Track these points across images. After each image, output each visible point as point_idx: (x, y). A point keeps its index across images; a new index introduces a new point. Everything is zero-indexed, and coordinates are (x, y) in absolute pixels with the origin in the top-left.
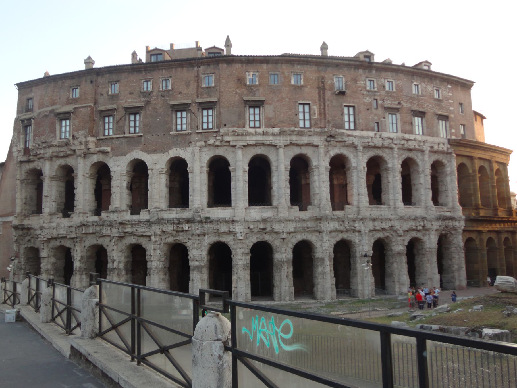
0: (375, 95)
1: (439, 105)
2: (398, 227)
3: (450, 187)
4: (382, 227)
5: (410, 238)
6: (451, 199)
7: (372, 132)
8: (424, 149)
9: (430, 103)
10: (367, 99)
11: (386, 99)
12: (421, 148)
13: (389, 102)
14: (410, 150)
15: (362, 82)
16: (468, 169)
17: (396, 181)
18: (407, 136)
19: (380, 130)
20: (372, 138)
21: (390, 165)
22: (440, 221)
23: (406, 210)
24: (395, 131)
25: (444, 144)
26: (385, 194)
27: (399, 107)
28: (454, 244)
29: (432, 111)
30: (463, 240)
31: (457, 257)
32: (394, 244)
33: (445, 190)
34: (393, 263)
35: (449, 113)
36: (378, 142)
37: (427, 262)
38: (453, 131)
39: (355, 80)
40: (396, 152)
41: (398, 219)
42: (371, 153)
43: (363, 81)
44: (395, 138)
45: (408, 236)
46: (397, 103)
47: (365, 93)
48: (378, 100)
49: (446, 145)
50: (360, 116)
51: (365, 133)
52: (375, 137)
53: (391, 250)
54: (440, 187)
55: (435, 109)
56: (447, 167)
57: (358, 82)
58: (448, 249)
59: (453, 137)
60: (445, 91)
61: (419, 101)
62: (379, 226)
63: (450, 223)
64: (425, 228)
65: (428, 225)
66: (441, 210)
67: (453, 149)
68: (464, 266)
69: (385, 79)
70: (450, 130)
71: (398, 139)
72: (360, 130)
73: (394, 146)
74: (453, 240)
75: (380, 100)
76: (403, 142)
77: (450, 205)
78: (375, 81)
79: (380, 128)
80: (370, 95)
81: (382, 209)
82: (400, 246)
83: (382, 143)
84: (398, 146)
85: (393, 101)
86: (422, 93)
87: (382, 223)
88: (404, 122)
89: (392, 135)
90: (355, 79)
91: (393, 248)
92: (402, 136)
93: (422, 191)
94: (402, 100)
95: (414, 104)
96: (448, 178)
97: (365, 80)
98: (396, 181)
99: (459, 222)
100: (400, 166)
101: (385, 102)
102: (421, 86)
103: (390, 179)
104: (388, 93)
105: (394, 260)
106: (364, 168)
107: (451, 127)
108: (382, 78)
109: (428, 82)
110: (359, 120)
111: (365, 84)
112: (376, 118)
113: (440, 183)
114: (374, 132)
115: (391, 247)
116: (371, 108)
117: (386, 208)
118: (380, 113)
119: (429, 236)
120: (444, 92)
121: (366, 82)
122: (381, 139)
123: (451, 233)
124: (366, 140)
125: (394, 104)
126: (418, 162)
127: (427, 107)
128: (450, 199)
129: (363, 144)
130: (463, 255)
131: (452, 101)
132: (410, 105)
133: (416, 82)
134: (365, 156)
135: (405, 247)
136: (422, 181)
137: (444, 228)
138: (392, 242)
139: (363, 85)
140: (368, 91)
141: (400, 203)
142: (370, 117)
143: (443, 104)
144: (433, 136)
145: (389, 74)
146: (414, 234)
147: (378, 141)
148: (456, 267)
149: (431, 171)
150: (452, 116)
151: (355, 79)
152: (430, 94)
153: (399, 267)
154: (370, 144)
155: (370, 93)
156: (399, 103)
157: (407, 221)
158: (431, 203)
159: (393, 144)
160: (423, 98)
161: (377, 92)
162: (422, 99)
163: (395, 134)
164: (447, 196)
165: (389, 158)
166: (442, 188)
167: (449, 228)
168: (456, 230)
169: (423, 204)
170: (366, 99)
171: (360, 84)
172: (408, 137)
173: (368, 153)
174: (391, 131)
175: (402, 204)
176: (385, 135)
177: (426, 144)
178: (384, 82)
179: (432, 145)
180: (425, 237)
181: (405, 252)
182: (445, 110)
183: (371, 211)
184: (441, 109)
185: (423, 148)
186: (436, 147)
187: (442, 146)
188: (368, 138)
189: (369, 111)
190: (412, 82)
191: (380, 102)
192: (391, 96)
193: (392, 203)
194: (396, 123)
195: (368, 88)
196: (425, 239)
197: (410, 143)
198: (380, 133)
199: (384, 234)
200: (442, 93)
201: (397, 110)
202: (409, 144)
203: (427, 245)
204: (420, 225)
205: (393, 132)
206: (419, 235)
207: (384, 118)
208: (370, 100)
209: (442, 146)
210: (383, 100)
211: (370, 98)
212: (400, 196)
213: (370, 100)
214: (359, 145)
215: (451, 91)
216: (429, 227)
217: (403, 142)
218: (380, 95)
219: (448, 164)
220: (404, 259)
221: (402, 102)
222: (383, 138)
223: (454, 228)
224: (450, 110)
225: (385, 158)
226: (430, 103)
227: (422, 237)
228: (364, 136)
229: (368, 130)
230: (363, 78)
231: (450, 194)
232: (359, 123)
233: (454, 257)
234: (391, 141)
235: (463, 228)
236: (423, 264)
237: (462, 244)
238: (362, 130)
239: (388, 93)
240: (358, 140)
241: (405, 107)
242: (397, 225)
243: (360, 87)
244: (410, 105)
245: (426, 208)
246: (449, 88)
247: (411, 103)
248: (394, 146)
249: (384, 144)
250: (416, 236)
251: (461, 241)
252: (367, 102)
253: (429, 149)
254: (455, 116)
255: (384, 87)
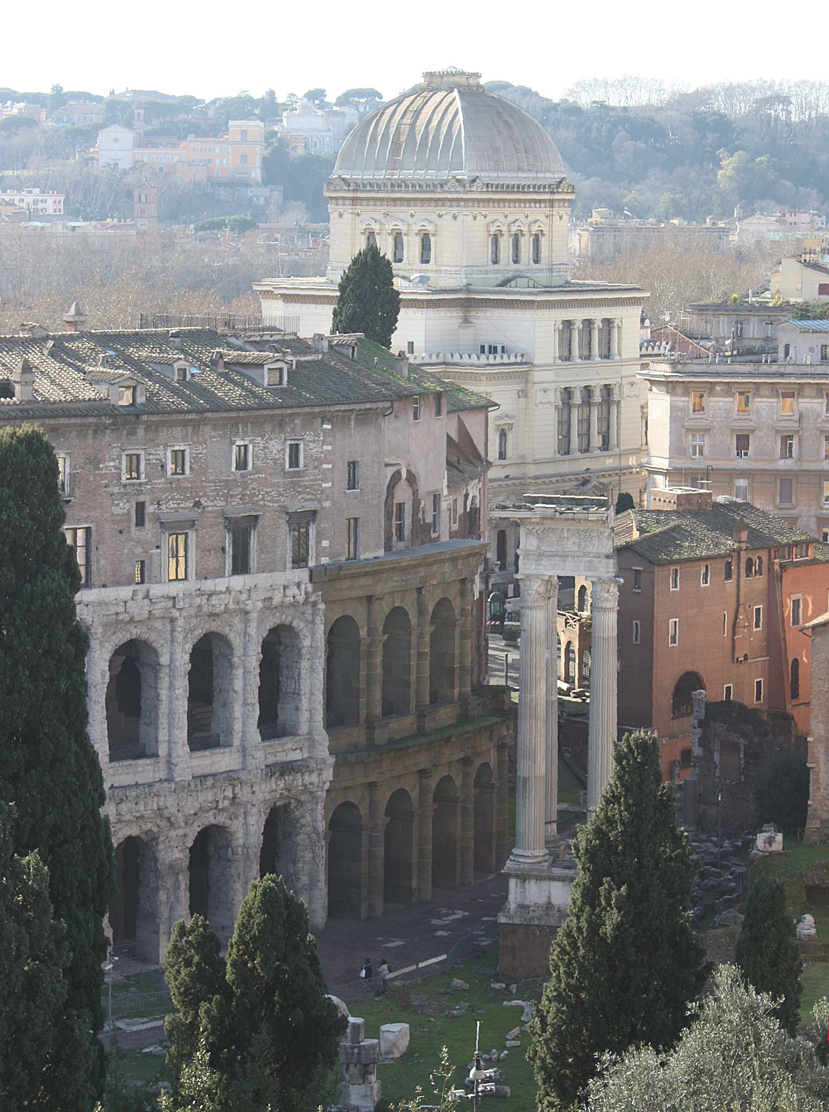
0: (139, 492)
1: (294, 485)
2: (173, 810)
3: (305, 687)
4: (138, 815)
5: (199, 829)
6: (307, 715)
7: (128, 588)
8: (249, 608)
9: (272, 485)
10: (121, 505)
11: (165, 499)
12: (242, 606)
13: (172, 504)
14: (213, 615)
15: (112, 464)
16: (357, 629)
17: (177, 699)
18: (209, 585)
19: (146, 578)
20: (126, 602)
21: (164, 660)
22: (273, 779)
23: (194, 763)
24: (181, 575)
25: (298, 585)
26: (149, 725)
27: (194, 515)
28: (303, 826)
29: (275, 505)
30: (325, 818)
31: (308, 856)
32: (161, 847)
33: (294, 693)
34: (157, 889)
35: (319, 501)
36: (139, 610)
37: (236, 879)
38: (325, 543)
39: (95, 462)
40: (179, 629)
41: (174, 791)
42: (122, 637)
43: (114, 460)
44: (181, 595)
45: (196, 824)
46: (192, 505)
47: (116, 490)
48: (147, 504)
49: (303, 587)
50: (100, 552)
51: (110, 593)
52: (132, 599)
53: (156, 860)
54: (283, 679)
55: (283, 499)
56: (302, 637)
57: (101, 466)
58: (290, 835)
59: (325, 560)
60: (314, 441)
61: (245, 487)
62: (130, 812)
63: (298, 781)
64: (237, 800)
65: (244, 794)
66: (280, 749)
67: (320, 593)
68: (322, 877)
69: (166, 446)
70: (318, 543)
71: (188, 595)
72: (99, 587)
73: (177, 614)
74: (302, 817)
75: (152, 504)
76: (198, 601)
77: (304, 728)
78: (142, 453)
79: (146, 574)
80: (126, 494)
81: (140, 769)
82: (176, 850)
83: (150, 612)
84: (185, 613)
85: (183, 500)
86: (254, 464)
87: (136, 803)
88: (204, 550)
89: (174, 589)
90: (95, 458)
91: (161, 855)
92: (197, 587)
93: (238, 710)
94: (205, 495)
95: (232, 496)
96: (305, 664)
97: (119, 458)
98: (177, 699)
99: (320, 774)
100: (187, 657)
101: (164, 507)
102: (254, 447)
103: (164, 693)
104: (171, 483)
105: (160, 883)
106: (103, 676)
107: (320, 537)
108: (158, 446)
109: (273, 431)
110: (98, 561)
111: (118, 468)
112: (139, 550)
113: (285, 672)
114: (132, 587)
115: (154, 853)
116: (129, 527)
117: (148, 765)
118: (150, 536)
119: (245, 818)
120: (312, 445)
121: (120, 463)
122: (147, 601)
123: (299, 801)
124: (113, 610)
125: (185, 508)
126: (232, 639)
127: (263, 499)
128: (304, 716)
129: (105, 619)
130: (323, 854)
131: (330, 466)
132: (224, 504)
133: (243, 439)
134: (107, 645)
135: (188, 851)
136: (238, 685)
137: (281, 794)
138: (157, 844)
139: (113, 471)
140: (125, 486)
141: (182, 749)
142: (126, 551)
143: (305, 481)
144: (272, 571)
145: (177, 432)
146: (210, 819)
147: (141, 608)
148: (305, 879)
149: (261, 656)
150: (327, 504)
151: (95, 458)
152: (275, 461)
153: (172, 899)
154: (120, 617)
155: (129, 489)
156: (197, 504)
157: (194, 794)
158: (254, 734)
159: (174, 611)
160: (256, 476)
161: (146, 483)
162: (253, 480)
163: (180, 585)
164: (297, 709)
165: (162, 642)
166: (287, 686)
167: (293, 792)
168: (311, 793)
169: (236, 742)
170: (118, 505)
171: (107, 467)
172: (212, 588)
173: (114, 637)
174: (173, 577)
175: (187, 749)
176: (156, 590)
177: (254, 596)
178: (165, 454)
179: (268, 595)
180: (235, 821)
181: (186, 863)
182: (309, 493)
183: (113, 775)
184: (299, 493)
185: (247, 605)
186: (277, 600)
187: (293, 590)
188: (117, 604)
189: (124, 536)
190: (233, 443)
191: (150, 509)
192: (178, 489)
193: (162, 750)
194: (186, 556)
195: (124, 477)
196: (236, 826)
197: (214, 600)
198: (144, 587)
199: (141, 827)
200: (305, 450)
201: (193, 523)
202: (213, 602)
203: (237, 839)
204: (225, 798)
205: (177, 579)
206: (222, 819)
207: (157, 547)
208: (127, 506)
209: (293, 590)
210: (158, 504)
211: (128, 501)
212: (182, 734)
213: (127, 506)
214: (96, 624)
215: (328, 440)
216: (245, 799)
217: (198, 601)
218: (152, 491)
219: (304, 631)
220: (184, 881)
221: (202, 501)
222: (150, 600)
223: (306, 789)
224: (323, 491)
225: (154, 644)
226: (272, 485)
227: (228, 822)
228: (107, 600)
229: (117, 583)
230: (115, 451)
231: (305, 704)
232: (98, 569)
233: (302, 857)
234: (170, 603)
235: (327, 785)
236: (227, 882)
237: (322, 826)
238: (104, 586)
239: (171, 483)
240: (94, 612)
241: (209, 512)
242: (171, 803)
243: (105, 476)
244: (224, 504)
245: (243, 750)
246: (324, 431)
247: (227, 497)
248: (177, 614)
249: (154, 612)
250: (214, 822)
251: (320, 817)
252: (121, 512)
253: (260, 604)
254: (333, 503)
255: (162, 466)
